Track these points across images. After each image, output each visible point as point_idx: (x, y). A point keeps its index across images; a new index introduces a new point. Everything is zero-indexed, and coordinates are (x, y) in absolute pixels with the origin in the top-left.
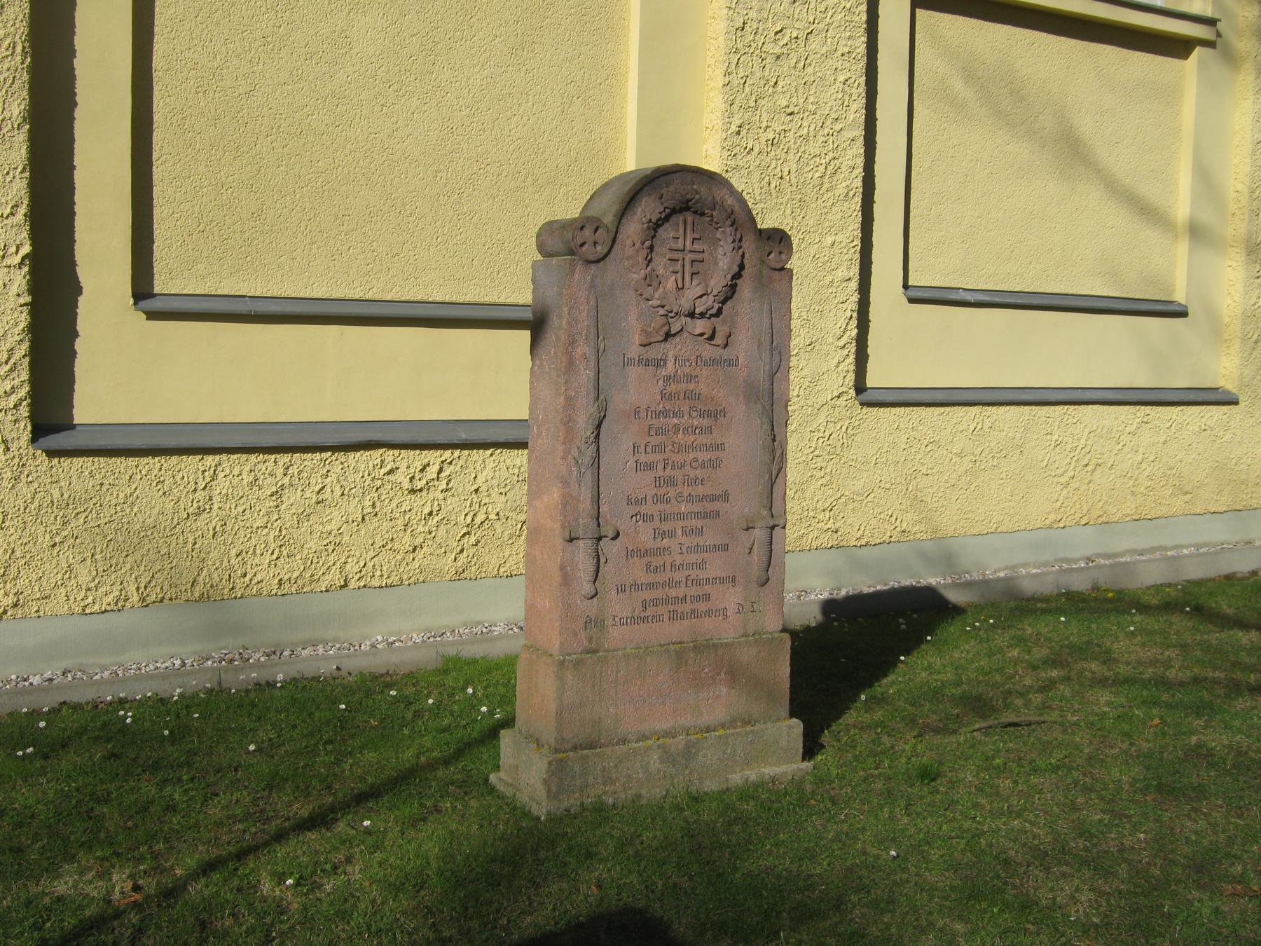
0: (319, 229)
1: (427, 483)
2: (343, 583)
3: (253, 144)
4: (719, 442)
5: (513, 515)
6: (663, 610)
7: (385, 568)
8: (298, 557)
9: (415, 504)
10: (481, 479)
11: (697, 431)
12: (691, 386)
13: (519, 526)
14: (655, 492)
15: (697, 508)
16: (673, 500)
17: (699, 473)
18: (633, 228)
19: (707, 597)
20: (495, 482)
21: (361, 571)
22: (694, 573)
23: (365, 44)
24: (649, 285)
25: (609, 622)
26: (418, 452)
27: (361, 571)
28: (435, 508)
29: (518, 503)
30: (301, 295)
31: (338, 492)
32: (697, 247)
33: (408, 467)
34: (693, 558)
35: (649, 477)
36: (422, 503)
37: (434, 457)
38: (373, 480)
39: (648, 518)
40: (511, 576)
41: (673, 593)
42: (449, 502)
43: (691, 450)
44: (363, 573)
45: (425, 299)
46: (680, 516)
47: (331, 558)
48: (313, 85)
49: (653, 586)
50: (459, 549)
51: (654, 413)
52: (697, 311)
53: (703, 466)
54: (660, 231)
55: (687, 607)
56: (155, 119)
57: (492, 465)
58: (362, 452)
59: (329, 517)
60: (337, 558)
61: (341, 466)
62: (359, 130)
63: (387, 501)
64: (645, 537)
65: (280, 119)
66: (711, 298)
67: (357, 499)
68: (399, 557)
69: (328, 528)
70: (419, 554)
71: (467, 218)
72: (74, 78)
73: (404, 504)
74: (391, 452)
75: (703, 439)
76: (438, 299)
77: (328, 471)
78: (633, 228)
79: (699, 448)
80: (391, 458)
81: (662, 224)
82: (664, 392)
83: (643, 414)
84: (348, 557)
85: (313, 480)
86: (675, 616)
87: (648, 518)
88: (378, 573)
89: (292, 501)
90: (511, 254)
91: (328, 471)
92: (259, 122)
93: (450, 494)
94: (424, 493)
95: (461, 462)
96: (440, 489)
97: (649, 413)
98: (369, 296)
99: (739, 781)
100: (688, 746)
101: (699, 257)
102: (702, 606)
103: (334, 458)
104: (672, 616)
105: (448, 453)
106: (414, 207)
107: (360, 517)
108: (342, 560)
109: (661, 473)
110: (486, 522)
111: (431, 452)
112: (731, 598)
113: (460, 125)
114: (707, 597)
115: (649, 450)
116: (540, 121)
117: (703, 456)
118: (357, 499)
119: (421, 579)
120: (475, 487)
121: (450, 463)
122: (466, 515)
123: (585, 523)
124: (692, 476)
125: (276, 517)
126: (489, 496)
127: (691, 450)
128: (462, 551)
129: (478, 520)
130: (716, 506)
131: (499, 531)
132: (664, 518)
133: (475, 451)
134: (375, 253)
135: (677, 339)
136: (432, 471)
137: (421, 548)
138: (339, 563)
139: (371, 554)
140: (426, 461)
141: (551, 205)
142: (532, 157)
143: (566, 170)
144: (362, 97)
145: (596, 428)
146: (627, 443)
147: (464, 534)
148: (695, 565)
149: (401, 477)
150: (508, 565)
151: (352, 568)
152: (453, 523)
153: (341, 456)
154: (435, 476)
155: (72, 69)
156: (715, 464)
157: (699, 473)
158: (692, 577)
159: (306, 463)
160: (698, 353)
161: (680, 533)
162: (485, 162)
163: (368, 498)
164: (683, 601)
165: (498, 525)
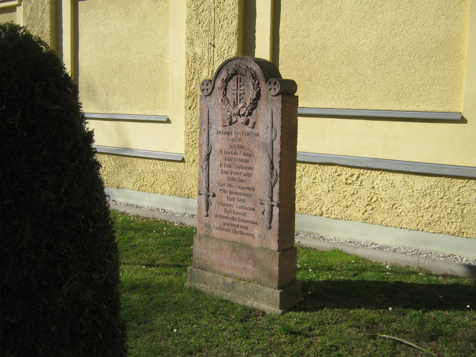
0: (330, 83)
1: (353, 181)
2: (320, 214)
3: (308, 54)
4: (251, 166)
5: (388, 200)
6: (230, 228)
7: (336, 212)
8: (306, 201)
9: (348, 189)
10: (375, 183)
11: (243, 161)
12: (241, 143)
13: (391, 206)
14: (228, 182)
15: (242, 191)
16: (234, 187)
17: (244, 178)
18: (219, 83)
19: (247, 228)
20: (381, 185)
21: (327, 211)
22: (242, 217)
23: (347, 10)
24: (224, 104)
25: (212, 227)
26: (350, 169)
27: (327, 211)
28: (355, 192)
29: (391, 196)
30: (323, 107)
31: (320, 180)
32: (242, 88)
33: (346, 174)
34: (241, 211)
35: (226, 176)
36: (350, 189)
37: (356, 171)
38: (333, 177)
39: (225, 192)
40: (387, 226)
41: (234, 222)
42: (361, 191)
43: (240, 168)
44: (328, 212)
45: (369, 108)
46: (237, 193)
47: (317, 204)
48: (329, 29)
49: (227, 218)
50: (365, 210)
51: (227, 152)
52: (241, 114)
53: (245, 175)
54: (229, 83)
55: (239, 229)
56: (280, 49)
57: (380, 178)
58: (330, 166)
59: (317, 189)
60: (319, 204)
61: (322, 171)
62: (345, 44)
63: (338, 186)
64: (224, 199)
65: (317, 43)
66: (245, 109)
67: (327, 184)
68: (341, 208)
69: (317, 193)
70: (349, 209)
71: (388, 75)
72: (255, 39)
73: (344, 188)
74: (340, 168)
75: (244, 164)
76: (375, 109)
77: (317, 172)
78: (219, 83)
79: (245, 168)
80: (340, 170)
81: (229, 80)
82: (231, 145)
83: (223, 152)
84: (323, 205)
85: (312, 175)
86: (234, 232)
87: (225, 192)
88: (333, 213)
89: (305, 181)
90: (407, 89)
91: (317, 172)
92: (310, 46)
93: (362, 187)
94: (352, 185)
95: (368, 175)
96: (358, 184)
97: (226, 152)
98: (348, 107)
99: (249, 305)
100: (233, 283)
101: (242, 92)
102: (245, 231)
103: (319, 167)
104: (233, 231)
105: (362, 170)
106: (365, 72)
107: (327, 190)
108: (321, 205)
109: (229, 176)
110: (377, 201)
111: (356, 169)
112: (256, 231)
113: (385, 36)
114: (247, 228)
115: (226, 166)
116: (423, 29)
117: (244, 171)
118: (327, 184)
119: (350, 219)
120: (372, 186)
121: (363, 175)
122: (368, 197)
123: (204, 190)
124: (241, 178)
125: (300, 186)
126: (379, 190)
127: (240, 168)
128: (366, 211)
129: (374, 199)
130: (250, 192)
131: (383, 206)
132: (231, 193)
133: (373, 171)
134: (350, 91)
135: (235, 125)
136: (355, 178)
137: (350, 206)
138: (320, 206)
139: (331, 205)
140: (353, 173)
141: (427, 66)
142: (418, 46)
143: (435, 50)
144: (346, 31)
145: (207, 156)
146: (218, 163)
147: (367, 205)
148: (242, 214)
149: (343, 178)
150: (386, 221)
151: (324, 209)
152: (363, 199)
153: (322, 167)
154: (355, 179)
155: (255, 37)
156: (249, 175)
157: (244, 178)
158: (241, 218)
159: (310, 168)
160: (243, 130)
161: (236, 199)
162: (396, 50)
163: (331, 184)
164: (238, 227)
165: (382, 203)
